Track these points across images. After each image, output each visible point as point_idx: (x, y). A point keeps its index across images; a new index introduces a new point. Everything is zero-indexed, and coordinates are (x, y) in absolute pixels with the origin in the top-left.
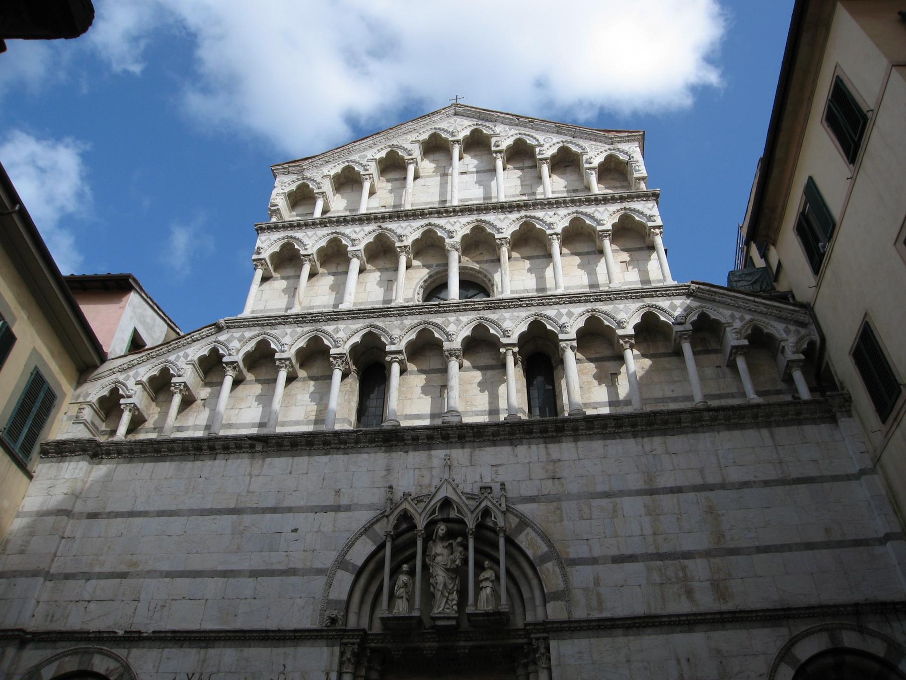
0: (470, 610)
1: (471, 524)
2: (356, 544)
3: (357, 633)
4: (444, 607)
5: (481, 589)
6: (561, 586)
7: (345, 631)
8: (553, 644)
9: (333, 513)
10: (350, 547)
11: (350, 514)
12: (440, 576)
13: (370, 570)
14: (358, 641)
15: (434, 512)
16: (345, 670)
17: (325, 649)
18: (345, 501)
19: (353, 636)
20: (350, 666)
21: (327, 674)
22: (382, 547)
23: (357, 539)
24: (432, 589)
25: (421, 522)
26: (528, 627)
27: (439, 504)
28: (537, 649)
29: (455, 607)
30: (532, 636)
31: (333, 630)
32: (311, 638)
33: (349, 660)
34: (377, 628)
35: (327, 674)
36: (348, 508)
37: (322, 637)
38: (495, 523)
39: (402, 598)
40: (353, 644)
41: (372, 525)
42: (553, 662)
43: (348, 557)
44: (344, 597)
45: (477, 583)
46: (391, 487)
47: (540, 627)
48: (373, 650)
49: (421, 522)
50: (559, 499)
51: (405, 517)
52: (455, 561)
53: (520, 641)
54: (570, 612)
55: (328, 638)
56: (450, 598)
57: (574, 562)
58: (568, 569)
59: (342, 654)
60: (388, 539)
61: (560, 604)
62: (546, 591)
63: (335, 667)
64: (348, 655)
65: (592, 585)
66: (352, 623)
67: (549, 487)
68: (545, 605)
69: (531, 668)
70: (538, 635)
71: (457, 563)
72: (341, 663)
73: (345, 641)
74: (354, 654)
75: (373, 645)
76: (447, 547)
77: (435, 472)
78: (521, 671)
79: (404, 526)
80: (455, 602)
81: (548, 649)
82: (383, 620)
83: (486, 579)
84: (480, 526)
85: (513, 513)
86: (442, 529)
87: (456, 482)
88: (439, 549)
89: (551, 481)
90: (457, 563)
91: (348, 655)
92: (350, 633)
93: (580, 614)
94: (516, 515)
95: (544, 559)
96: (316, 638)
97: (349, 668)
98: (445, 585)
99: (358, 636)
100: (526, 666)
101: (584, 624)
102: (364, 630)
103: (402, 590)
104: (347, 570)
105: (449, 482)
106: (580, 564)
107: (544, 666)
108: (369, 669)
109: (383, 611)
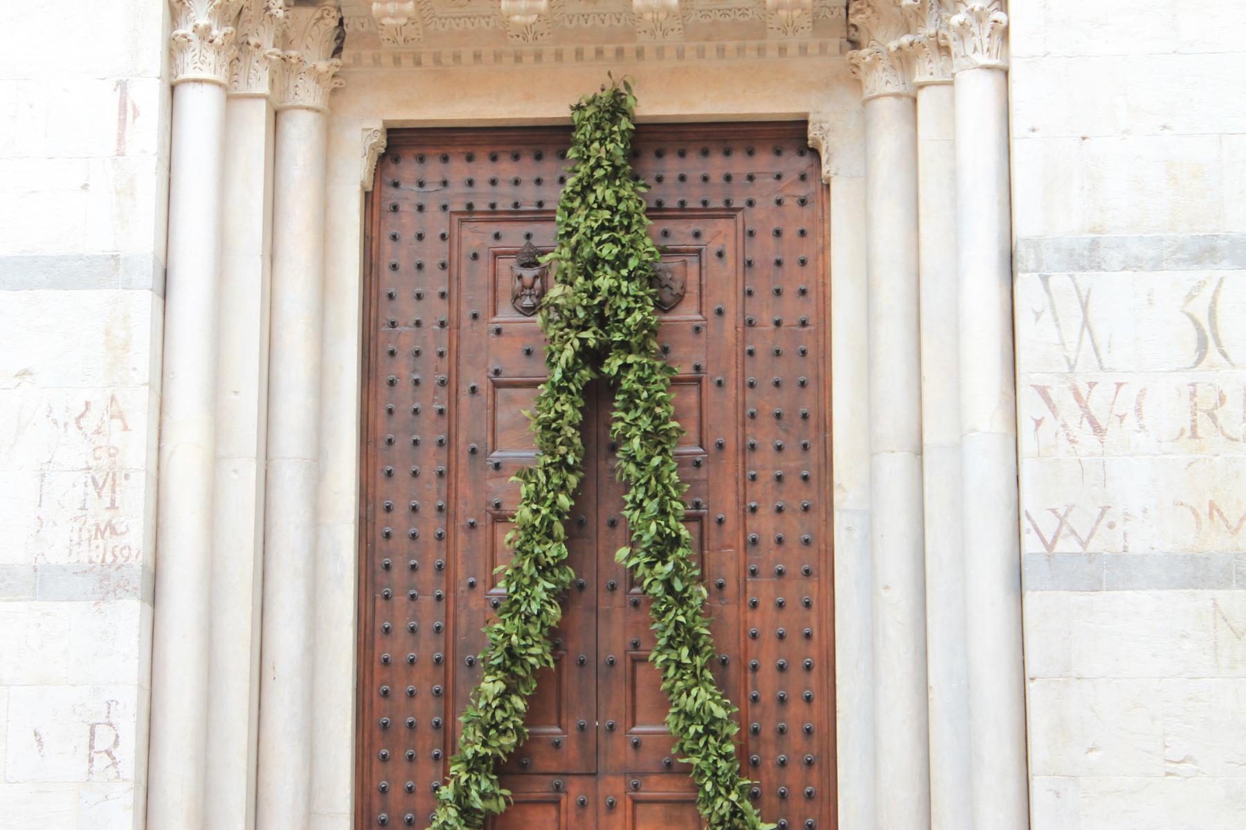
16: (190, 74)
20: (211, 57)
21: (122, 86)
33: (204, 34)
35: (122, 86)
72: (174, 49)
78: (882, 81)
97: (202, 64)
100: (904, 60)
107: (983, 59)
108: (285, 68)
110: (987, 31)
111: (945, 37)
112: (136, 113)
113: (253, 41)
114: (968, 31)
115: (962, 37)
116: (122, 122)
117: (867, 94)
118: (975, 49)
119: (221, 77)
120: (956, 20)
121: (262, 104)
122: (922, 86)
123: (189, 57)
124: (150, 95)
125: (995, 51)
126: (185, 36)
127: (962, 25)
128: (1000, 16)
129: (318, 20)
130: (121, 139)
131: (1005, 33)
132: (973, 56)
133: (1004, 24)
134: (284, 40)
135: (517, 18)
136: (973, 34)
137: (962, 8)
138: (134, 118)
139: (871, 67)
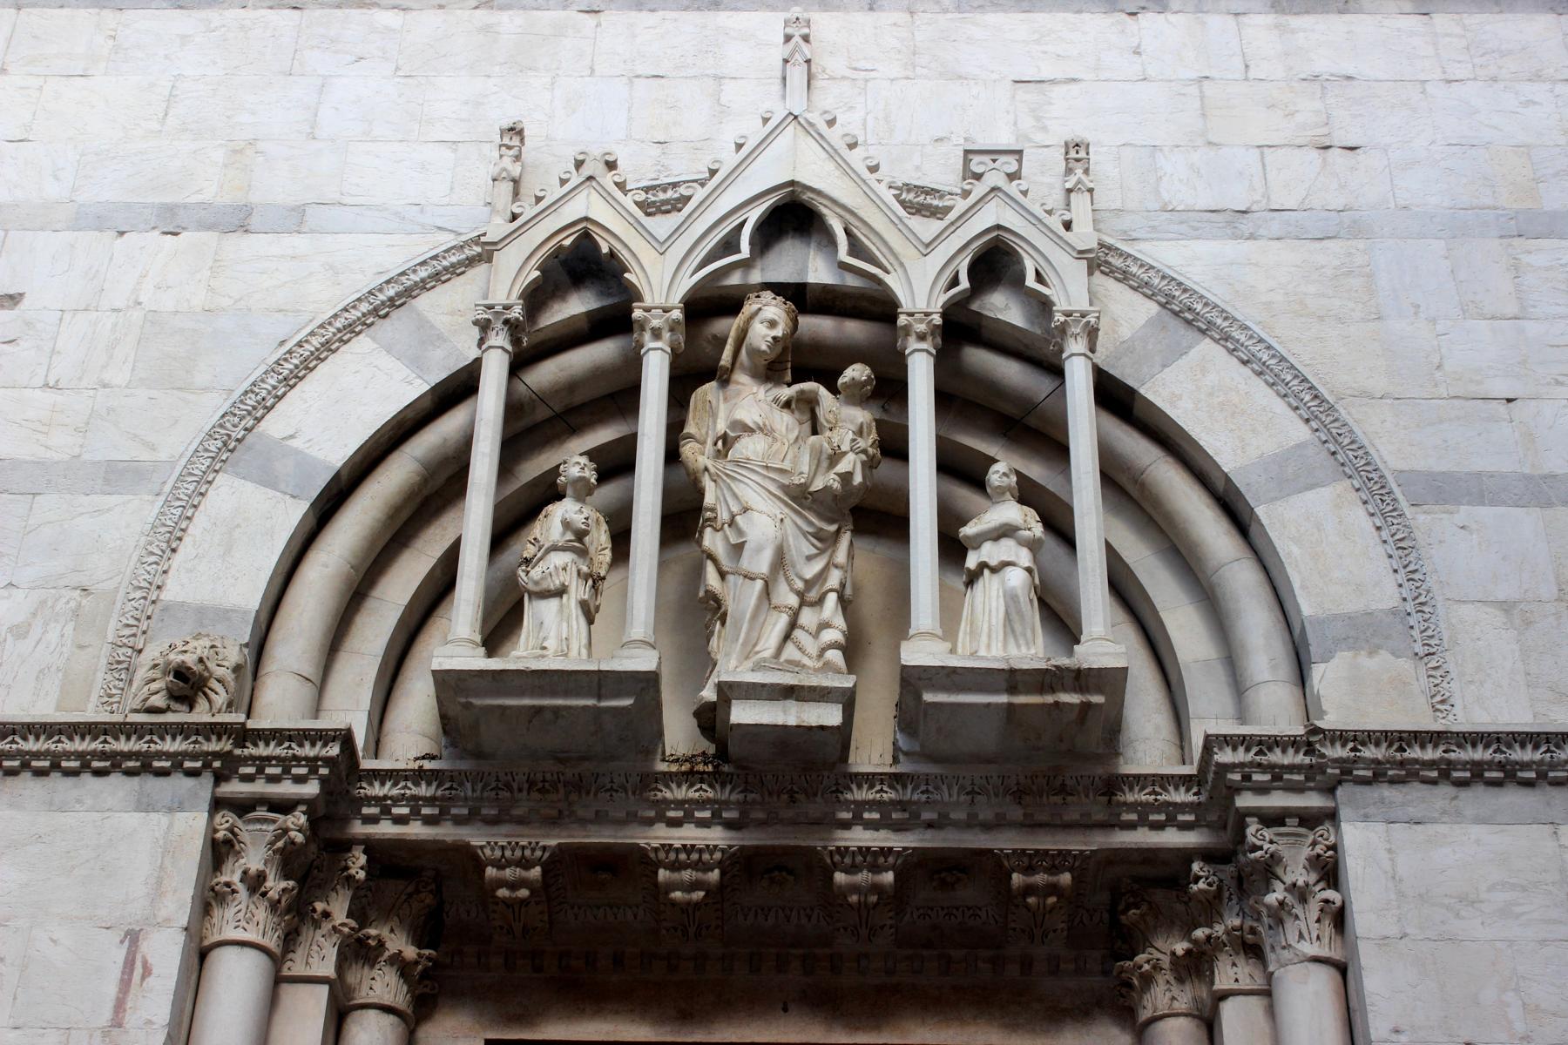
0: (920, 652)
1: (920, 289)
2: (323, 369)
3: (308, 751)
4: (777, 652)
5: (972, 578)
6: (1386, 594)
7: (243, 735)
8: (1361, 839)
9: (210, 237)
10: (291, 381)
11: (300, 243)
12: (756, 516)
13: (395, 490)
14: (312, 789)
15: (729, 245)
17: (133, 819)
18: (274, 186)
19: (286, 763)
20: (261, 913)
21: (133, 938)
22: (459, 388)
23: (328, 348)
24: (712, 578)
25: (662, 279)
26: (1225, 756)
27: (754, 215)
28: (1269, 870)
29: (835, 656)
30: (1245, 801)
31: (183, 730)
32: (54, 766)
33: (255, 883)
34: (412, 734)
35: (133, 938)
36: (296, 219)
37: (114, 764)
38: (1043, 306)
39: (560, 592)
40: (284, 806)
41: (409, 293)
42: (1362, 920)
43: (274, 426)
44: (250, 596)
45: (952, 548)
46: (516, 131)
47: (1290, 758)
48: (384, 857)
49: (662, 279)
50: (1357, 230)
51: (582, 262)
52: (835, 457)
53: (1172, 838)
54: (1441, 703)
55: (145, 766)
56: (808, 617)
57: (1445, 490)
58: (1420, 520)
59: (219, 851)
60: (499, 338)
61: (1379, 664)
62: (1307, 606)
63: (179, 902)
64: (254, 857)
65: (1548, 591)
66: (280, 703)
67: (1297, 179)
68: (1301, 676)
69: (1230, 973)
70: (1278, 800)
71: (843, 467)
73: (234, 788)
74: (288, 859)
75: (386, 829)
76: (787, 405)
77: (730, 92)
78: (1163, 996)
79: (576, 305)
80: (833, 635)
81: (1330, 871)
82: (449, 684)
83: (1004, 532)
84: (959, 328)
85: (1124, 277)
86: (766, 321)
87: (849, 122)
88: (749, 401)
89: (1315, 154)
90: (843, 467)
91: (254, 857)
92: (272, 750)
93: (1494, 702)
94: (1142, 288)
95: (1291, 476)
96: (86, 766)
97: (246, 920)
98: (780, 561)
99: (312, 763)
100: (1195, 966)
101: (1528, 755)
102: (345, 738)
103: (559, 559)
104: (268, 480)
105: (809, 128)
106: (1481, 498)
109: (455, 644)
110: (1315, 914)
111: (1253, 931)
112: (147, 971)
113: (320, 906)
114: (1290, 913)
115: (1281, 922)
116: (125, 984)
117: (1144, 1015)
118: (1301, 936)
119: (272, 942)
120: (1272, 898)
121: (324, 990)
122: (1224, 996)
123: (230, 912)
124: (166, 953)
125: (1326, 940)
126: (228, 885)
127: (1282, 904)
128: (1330, 894)
129: (410, 895)
130: (120, 1006)
131: (1339, 919)
132: (1299, 946)
133: (1338, 903)
134: (359, 913)
135: (677, 895)
136: (1297, 917)
137: (1278, 886)
138: (143, 978)
139: (1148, 980)
